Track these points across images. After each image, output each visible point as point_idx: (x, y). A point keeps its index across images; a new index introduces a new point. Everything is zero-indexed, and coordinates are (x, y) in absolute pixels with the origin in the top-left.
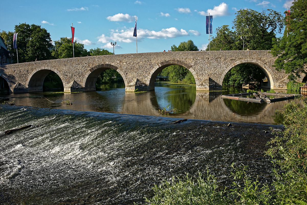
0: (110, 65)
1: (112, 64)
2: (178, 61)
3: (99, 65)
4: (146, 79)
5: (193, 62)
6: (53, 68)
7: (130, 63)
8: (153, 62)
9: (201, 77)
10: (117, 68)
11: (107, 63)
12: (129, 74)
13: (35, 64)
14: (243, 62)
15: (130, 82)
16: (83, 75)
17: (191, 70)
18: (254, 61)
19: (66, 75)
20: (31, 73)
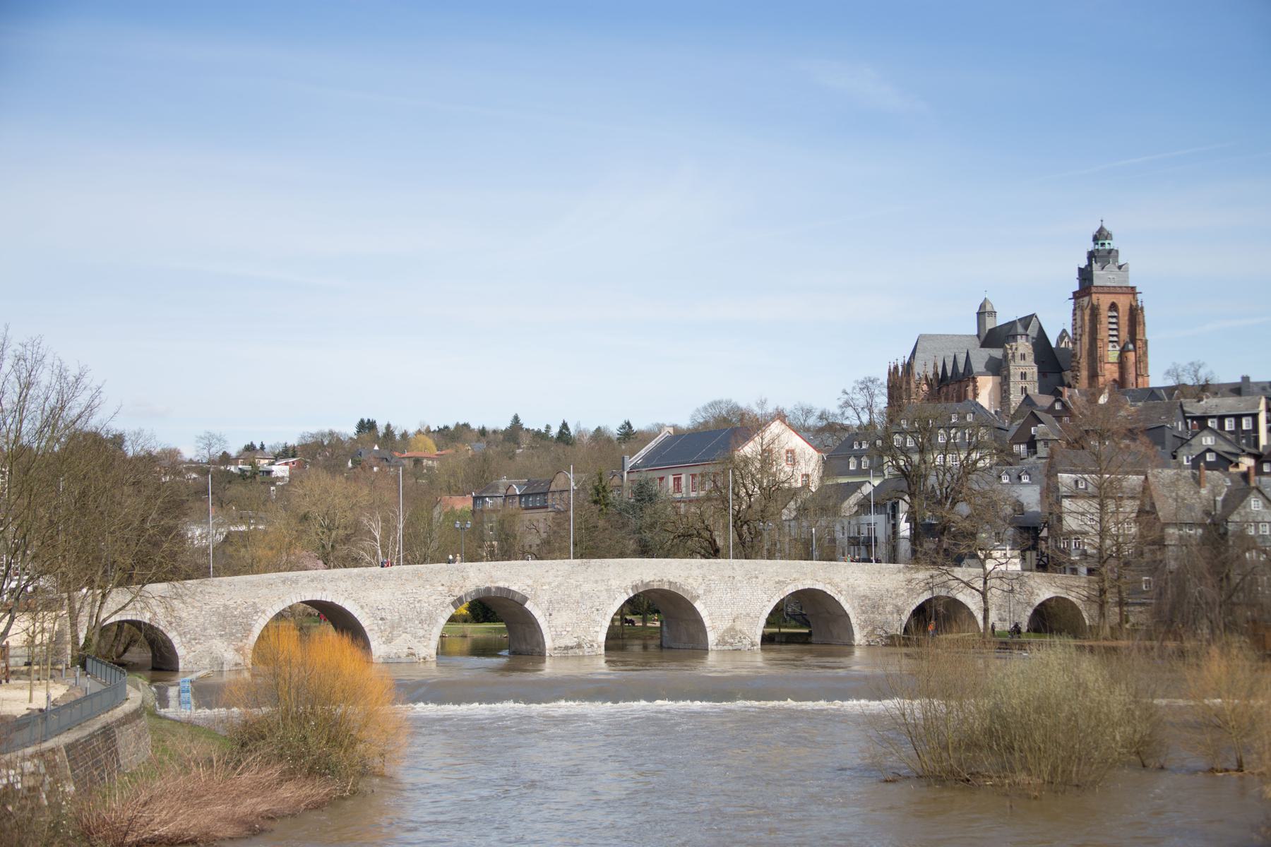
0: (509, 591)
1: (514, 588)
2: (670, 583)
3: (478, 591)
4: (597, 629)
5: (703, 587)
6: (342, 598)
7: (558, 586)
8: (614, 583)
9: (717, 623)
10: (526, 599)
11: (501, 584)
12: (554, 613)
13: (284, 582)
14: (800, 587)
15: (559, 635)
16: (431, 619)
17: (698, 605)
18: (819, 586)
19: (382, 619)
20: (264, 612)
